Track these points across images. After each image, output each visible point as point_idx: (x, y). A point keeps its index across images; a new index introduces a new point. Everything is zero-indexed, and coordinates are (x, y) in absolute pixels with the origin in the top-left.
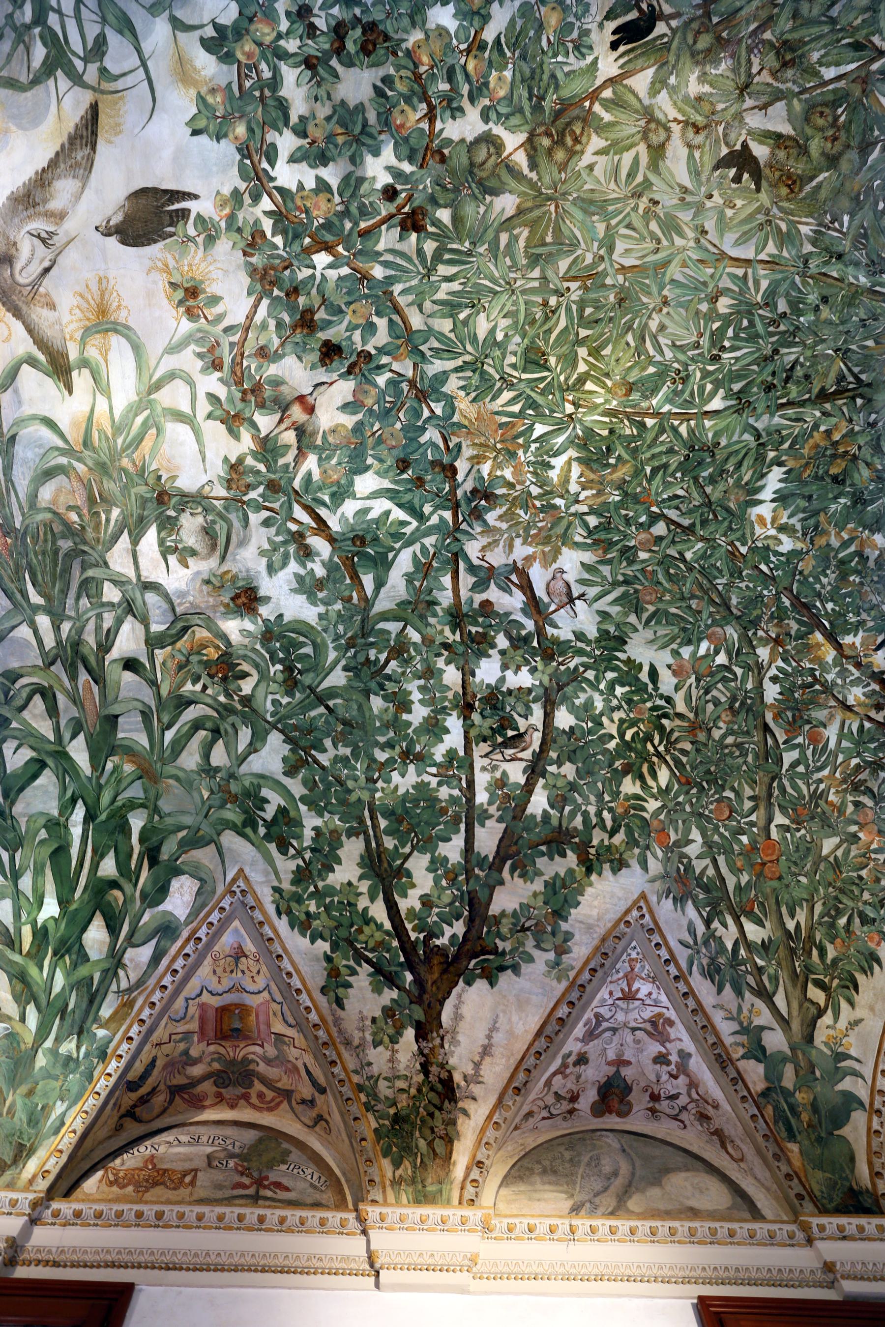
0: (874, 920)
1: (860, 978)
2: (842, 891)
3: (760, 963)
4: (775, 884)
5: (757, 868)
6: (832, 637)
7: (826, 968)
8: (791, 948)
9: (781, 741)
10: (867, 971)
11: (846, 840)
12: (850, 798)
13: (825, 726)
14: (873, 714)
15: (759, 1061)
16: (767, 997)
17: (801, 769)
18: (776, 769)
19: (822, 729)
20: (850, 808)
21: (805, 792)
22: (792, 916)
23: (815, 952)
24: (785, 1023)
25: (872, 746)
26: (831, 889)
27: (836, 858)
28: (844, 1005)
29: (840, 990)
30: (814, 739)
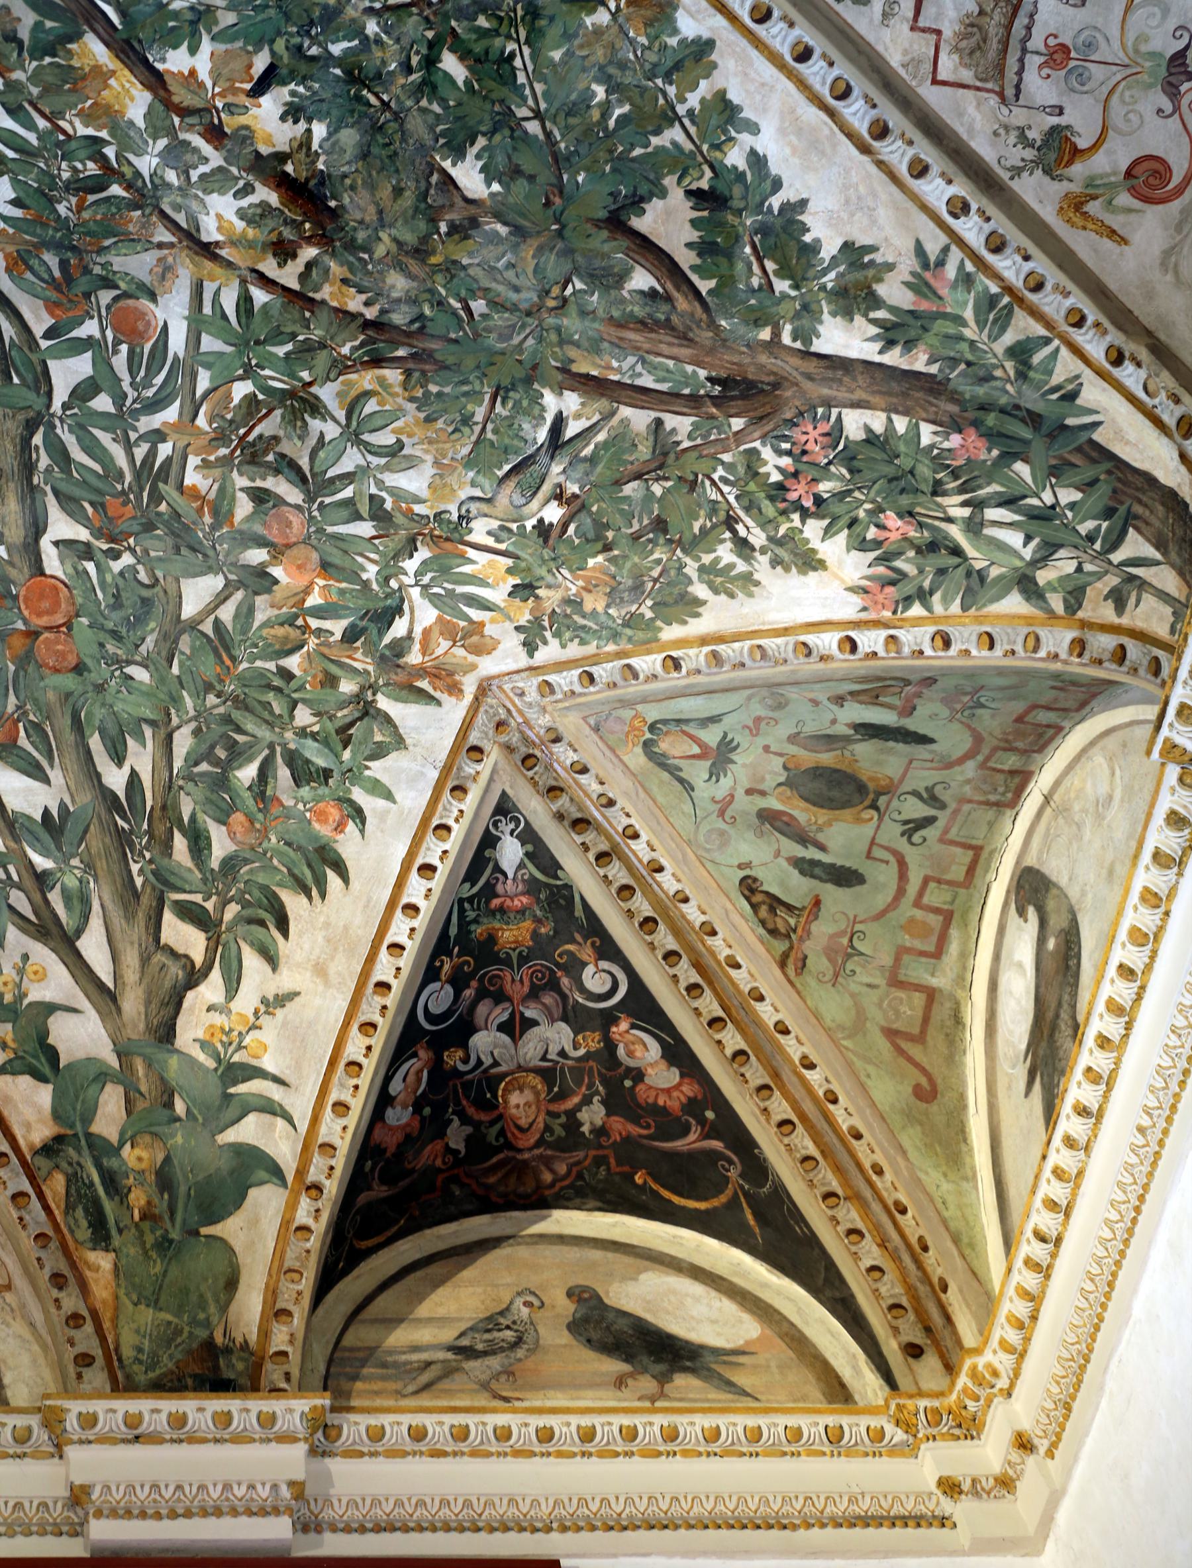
0: (327, 774)
1: (294, 903)
2: (240, 703)
3: (42, 862)
4: (69, 682)
5: (18, 642)
6: (131, 52)
7: (209, 880)
8: (119, 832)
9: (38, 330)
10: (311, 888)
11: (240, 584)
12: (241, 482)
13: (153, 297)
14: (269, 266)
15: (41, 1078)
16: (65, 943)
17: (103, 403)
18: (39, 403)
19: (145, 303)
20: (244, 507)
21: (122, 461)
22: (119, 759)
23: (180, 843)
24: (106, 997)
25: (281, 351)
26: (211, 699)
27: (217, 623)
28: (252, 961)
29: (241, 929)
30: (130, 328)
